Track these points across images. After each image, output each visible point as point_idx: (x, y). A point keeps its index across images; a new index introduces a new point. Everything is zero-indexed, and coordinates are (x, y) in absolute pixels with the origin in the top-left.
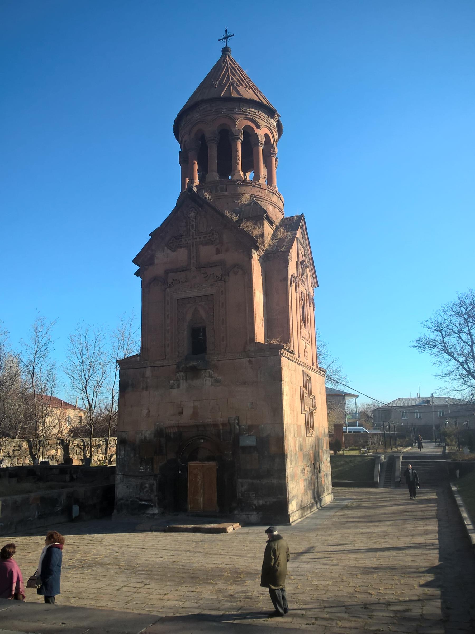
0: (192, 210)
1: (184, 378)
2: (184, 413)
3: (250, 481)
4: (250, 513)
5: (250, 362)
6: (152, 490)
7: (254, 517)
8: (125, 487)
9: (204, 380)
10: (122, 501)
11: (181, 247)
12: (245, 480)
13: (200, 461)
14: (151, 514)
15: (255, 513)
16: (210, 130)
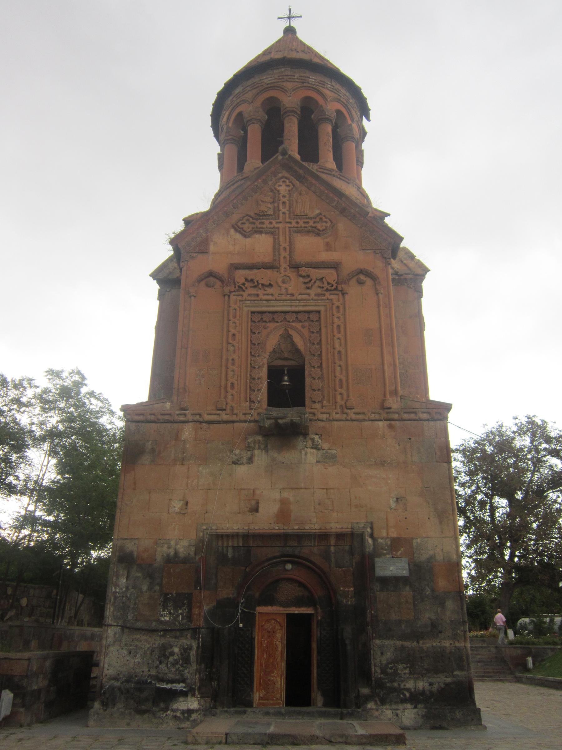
0: (284, 182)
1: (262, 446)
2: (260, 509)
3: (399, 643)
4: (401, 706)
5: (391, 427)
6: (186, 660)
7: (409, 714)
8: (125, 652)
9: (303, 452)
10: (117, 684)
11: (261, 232)
12: (387, 642)
13: (281, 605)
14: (183, 712)
15: (409, 706)
16: (290, 100)
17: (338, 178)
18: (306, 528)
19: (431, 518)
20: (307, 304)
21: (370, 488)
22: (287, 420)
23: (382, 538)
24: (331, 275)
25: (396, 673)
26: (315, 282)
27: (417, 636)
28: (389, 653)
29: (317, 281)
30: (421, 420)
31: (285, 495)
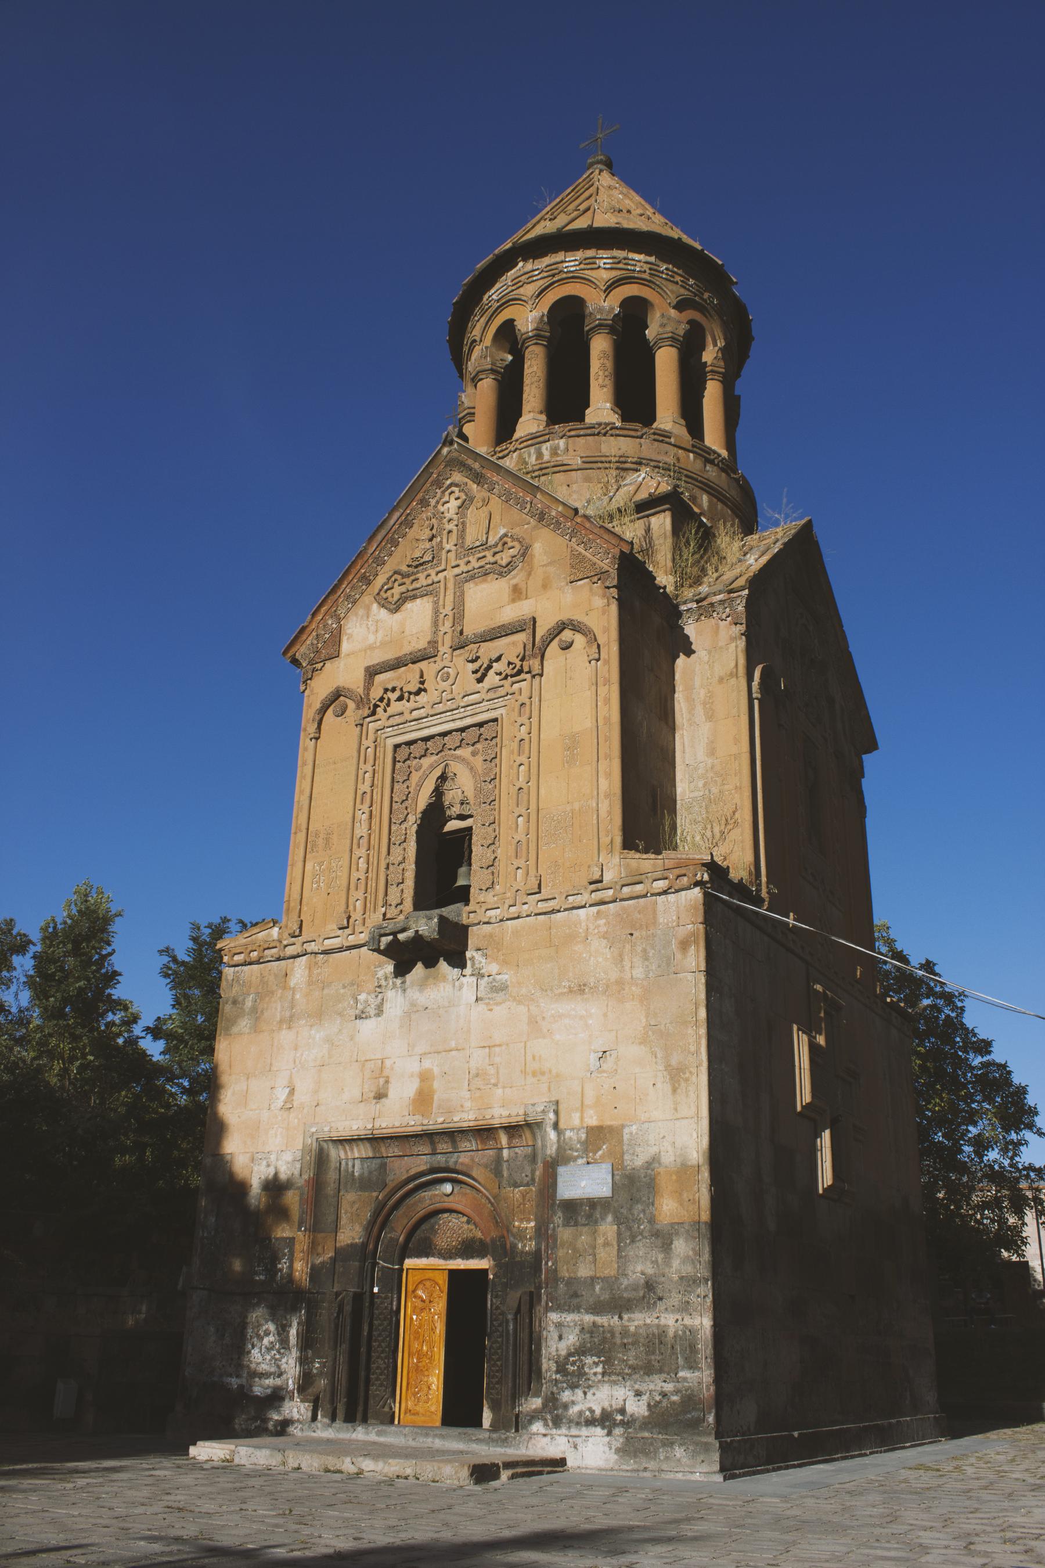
2: (392, 1093)
3: (588, 1318)
4: (584, 1431)
11: (415, 597)
12: (570, 1318)
15: (599, 1431)
17: (612, 435)
18: (455, 1119)
19: (659, 1085)
20: (478, 711)
21: (557, 1037)
22: (410, 933)
23: (572, 1129)
24: (511, 647)
25: (581, 1373)
26: (490, 667)
27: (619, 1305)
28: (571, 1337)
29: (494, 664)
30: (652, 895)
31: (427, 1064)
